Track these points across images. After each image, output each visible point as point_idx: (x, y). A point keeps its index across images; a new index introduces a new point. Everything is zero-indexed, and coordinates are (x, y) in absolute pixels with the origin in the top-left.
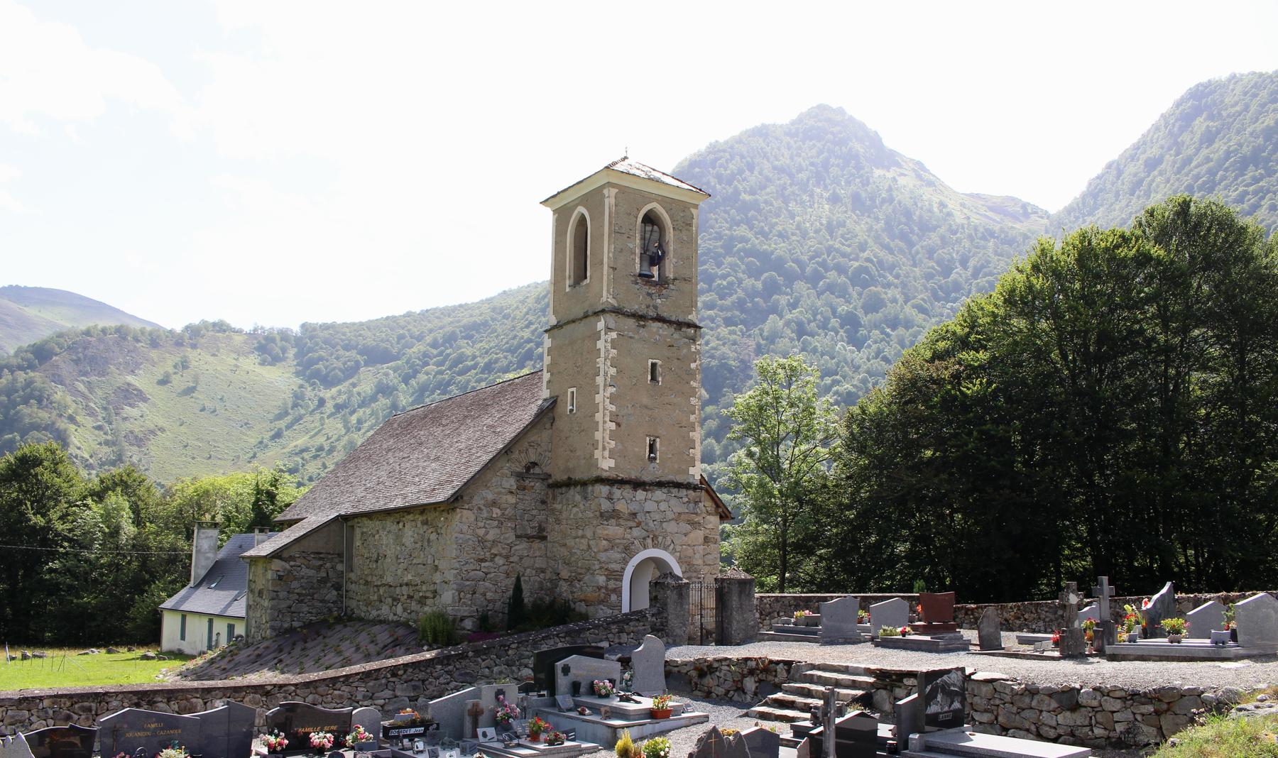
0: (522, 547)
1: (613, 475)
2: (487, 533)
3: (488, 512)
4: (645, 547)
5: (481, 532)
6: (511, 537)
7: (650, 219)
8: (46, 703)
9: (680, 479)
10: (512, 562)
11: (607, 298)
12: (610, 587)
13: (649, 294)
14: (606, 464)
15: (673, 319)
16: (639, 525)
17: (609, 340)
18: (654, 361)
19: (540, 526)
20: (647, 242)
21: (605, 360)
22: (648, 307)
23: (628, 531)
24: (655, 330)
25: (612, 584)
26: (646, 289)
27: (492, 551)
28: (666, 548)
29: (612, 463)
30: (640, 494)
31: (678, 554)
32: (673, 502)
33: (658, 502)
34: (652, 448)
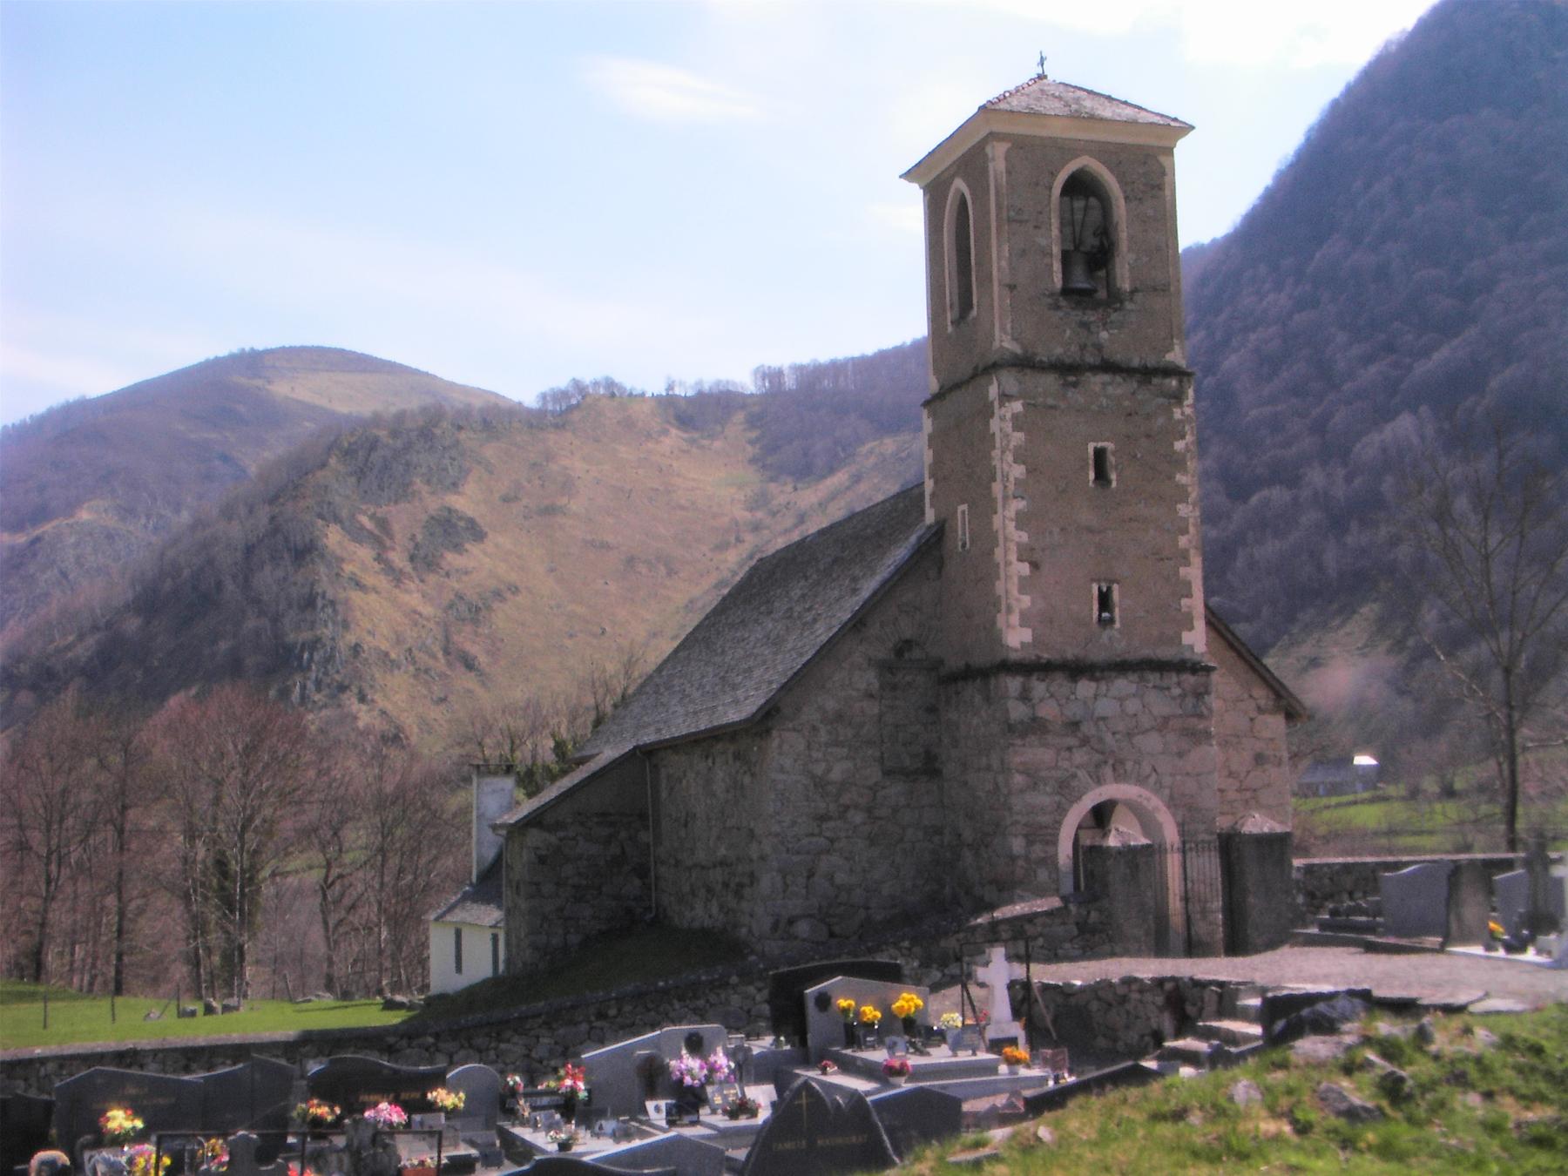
0: (895, 791)
1: (1030, 655)
2: (829, 770)
3: (830, 733)
4: (1099, 781)
5: (819, 769)
6: (874, 774)
7: (1080, 186)
8: (51, 1067)
9: (1166, 653)
10: (880, 818)
11: (1005, 342)
12: (1033, 856)
13: (1085, 325)
14: (1016, 637)
15: (1136, 362)
16: (1085, 742)
17: (1009, 416)
18: (1100, 445)
19: (927, 752)
20: (1078, 229)
21: (1003, 452)
22: (1083, 348)
23: (1065, 754)
24: (1097, 389)
25: (1038, 851)
26: (1077, 316)
27: (842, 801)
28: (1141, 781)
29: (1026, 635)
30: (1085, 688)
31: (1167, 792)
32: (1153, 697)
33: (1121, 700)
34: (1105, 601)
